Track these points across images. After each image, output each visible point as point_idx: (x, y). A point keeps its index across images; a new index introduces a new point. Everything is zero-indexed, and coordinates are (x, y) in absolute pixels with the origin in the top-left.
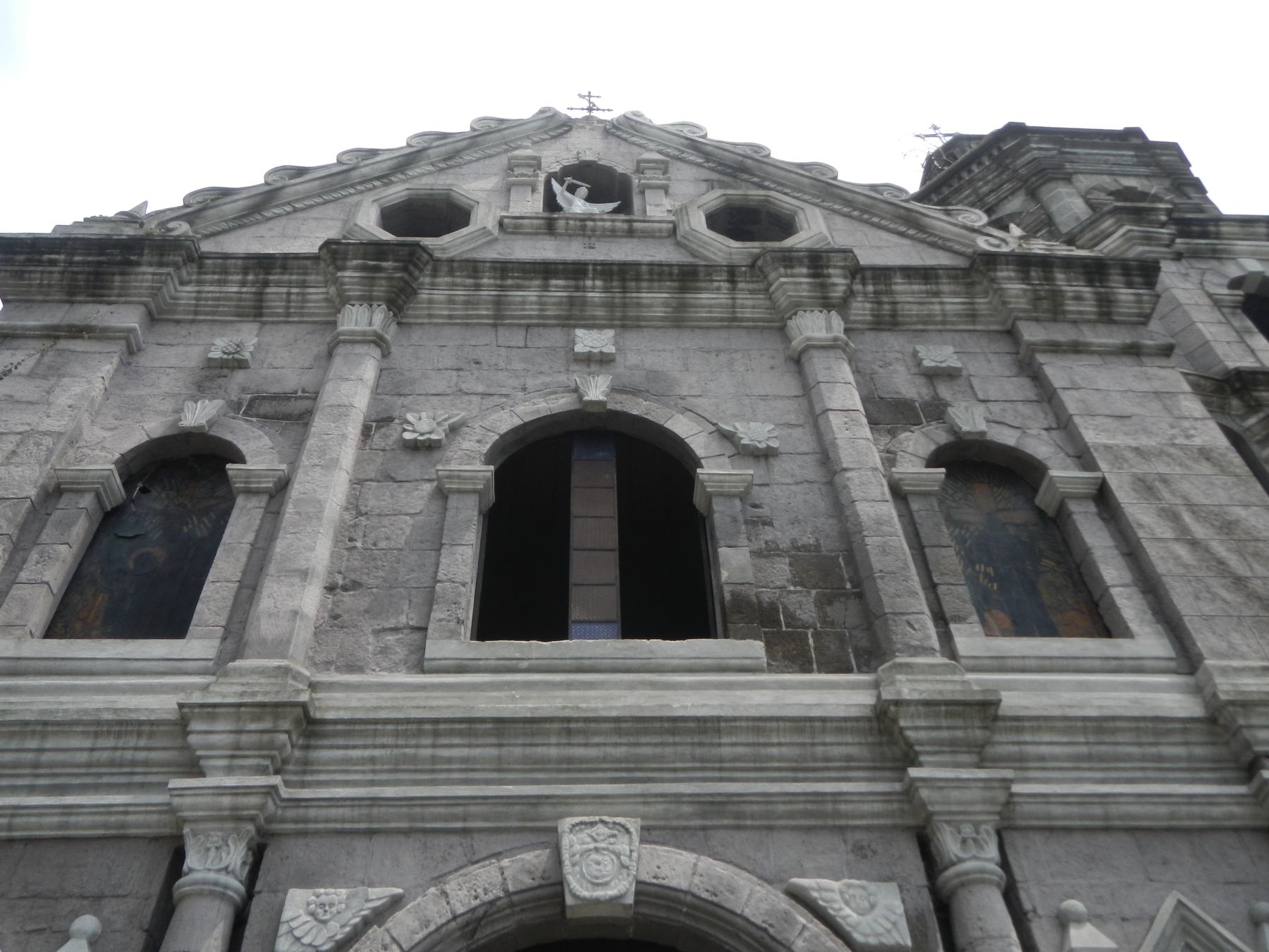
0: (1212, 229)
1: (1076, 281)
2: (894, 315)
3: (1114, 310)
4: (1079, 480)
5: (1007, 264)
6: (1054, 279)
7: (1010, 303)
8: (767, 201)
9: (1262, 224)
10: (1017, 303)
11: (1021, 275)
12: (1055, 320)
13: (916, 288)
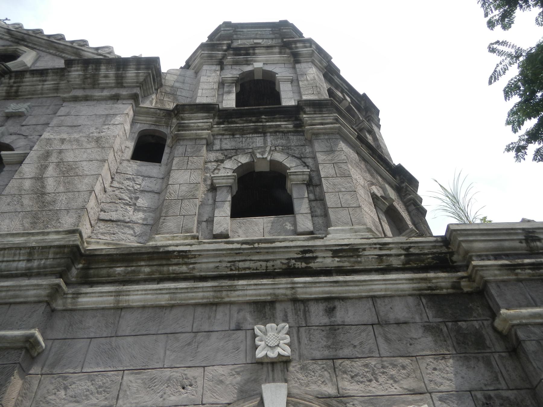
0: (251, 51)
1: (111, 69)
2: (17, 92)
3: (124, 81)
4: (19, 155)
5: (78, 64)
6: (100, 70)
7: (71, 81)
8: (16, 51)
9: (277, 48)
10: (75, 81)
11: (83, 68)
12: (94, 88)
13: (35, 79)
